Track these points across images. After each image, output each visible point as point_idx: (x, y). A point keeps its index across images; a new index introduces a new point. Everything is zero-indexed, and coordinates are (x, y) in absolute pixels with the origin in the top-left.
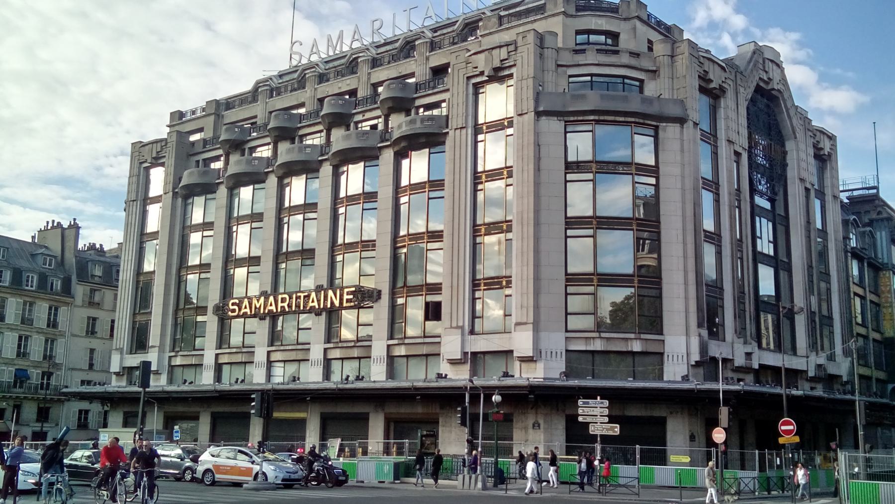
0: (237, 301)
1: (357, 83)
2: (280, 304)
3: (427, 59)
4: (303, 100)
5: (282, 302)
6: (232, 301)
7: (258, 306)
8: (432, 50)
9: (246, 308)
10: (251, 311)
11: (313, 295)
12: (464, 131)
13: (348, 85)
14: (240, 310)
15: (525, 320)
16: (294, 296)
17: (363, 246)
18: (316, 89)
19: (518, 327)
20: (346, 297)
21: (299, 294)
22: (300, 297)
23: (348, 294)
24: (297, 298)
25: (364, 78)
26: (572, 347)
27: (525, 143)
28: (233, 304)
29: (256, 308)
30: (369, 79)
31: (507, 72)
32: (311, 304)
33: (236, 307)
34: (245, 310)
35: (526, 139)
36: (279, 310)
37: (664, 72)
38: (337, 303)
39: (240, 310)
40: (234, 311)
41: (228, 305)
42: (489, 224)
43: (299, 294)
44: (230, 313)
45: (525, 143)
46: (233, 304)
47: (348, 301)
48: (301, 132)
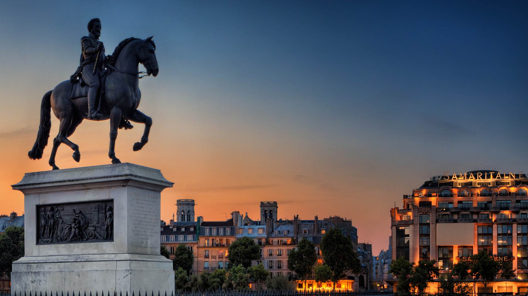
0: (466, 257)
1: (492, 199)
3: (515, 197)
4: (471, 200)
6: (464, 257)
9: (469, 259)
13: (489, 199)
20: (505, 259)
23: (505, 258)
25: (495, 198)
28: (464, 258)
30: (496, 199)
38: (502, 260)
39: (467, 259)
40: (465, 260)
44: (463, 260)
46: (464, 258)
47: (505, 260)
48: (481, 213)
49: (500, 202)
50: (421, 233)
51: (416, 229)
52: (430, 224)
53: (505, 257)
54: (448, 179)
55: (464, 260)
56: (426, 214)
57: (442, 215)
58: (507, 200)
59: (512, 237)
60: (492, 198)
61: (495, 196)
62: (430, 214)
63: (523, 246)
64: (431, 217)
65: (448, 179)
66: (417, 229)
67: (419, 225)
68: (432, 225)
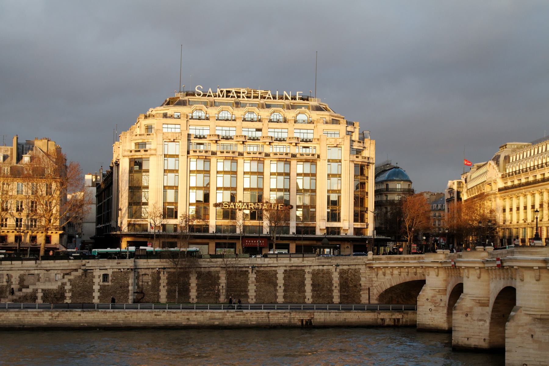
0: (227, 203)
2: (249, 206)
3: (294, 125)
5: (250, 205)
7: (238, 206)
8: (295, 122)
9: (232, 206)
10: (235, 207)
11: (265, 204)
12: (325, 161)
14: (229, 206)
15: (346, 219)
16: (256, 204)
17: (285, 190)
18: (241, 123)
19: (344, 221)
21: (258, 204)
22: (259, 205)
23: (280, 206)
24: (257, 205)
26: (355, 227)
27: (347, 169)
28: (225, 204)
29: (237, 206)
31: (340, 146)
32: (264, 208)
33: (228, 206)
34: (232, 207)
35: (347, 168)
36: (249, 208)
37: (368, 148)
39: (229, 206)
40: (226, 207)
41: (223, 204)
42: (333, 190)
43: (258, 204)
44: (224, 207)
45: (347, 169)
46: (225, 204)
47: (281, 208)
49: (273, 130)
50: (166, 168)
51: (159, 162)
52: (180, 156)
53: (279, 205)
54: (201, 96)
55: (225, 207)
56: (174, 141)
57: (196, 144)
58: (282, 129)
59: (290, 179)
60: (263, 124)
61: (267, 122)
62: (179, 142)
63: (304, 191)
64: (180, 146)
65: (201, 96)
66: (161, 162)
67: (163, 156)
68: (182, 157)
